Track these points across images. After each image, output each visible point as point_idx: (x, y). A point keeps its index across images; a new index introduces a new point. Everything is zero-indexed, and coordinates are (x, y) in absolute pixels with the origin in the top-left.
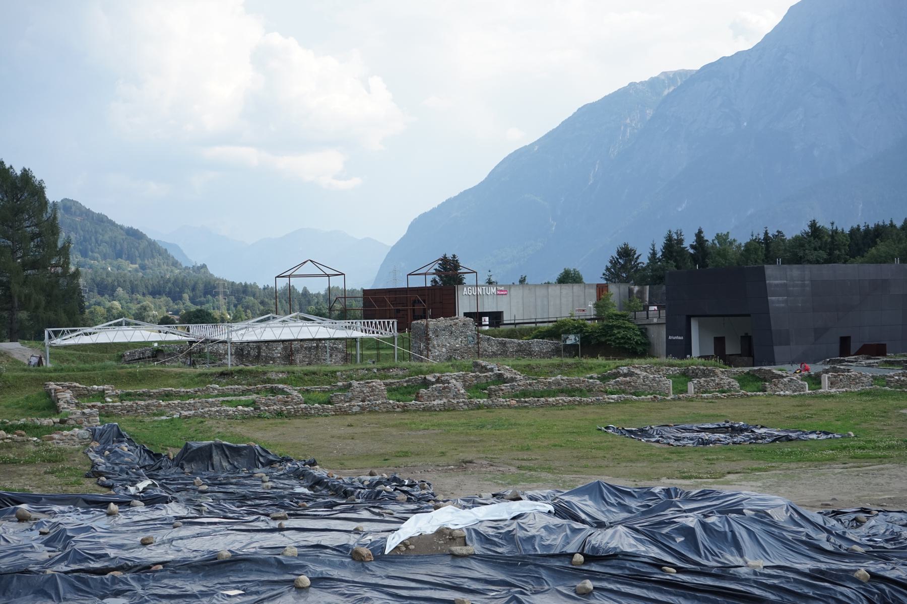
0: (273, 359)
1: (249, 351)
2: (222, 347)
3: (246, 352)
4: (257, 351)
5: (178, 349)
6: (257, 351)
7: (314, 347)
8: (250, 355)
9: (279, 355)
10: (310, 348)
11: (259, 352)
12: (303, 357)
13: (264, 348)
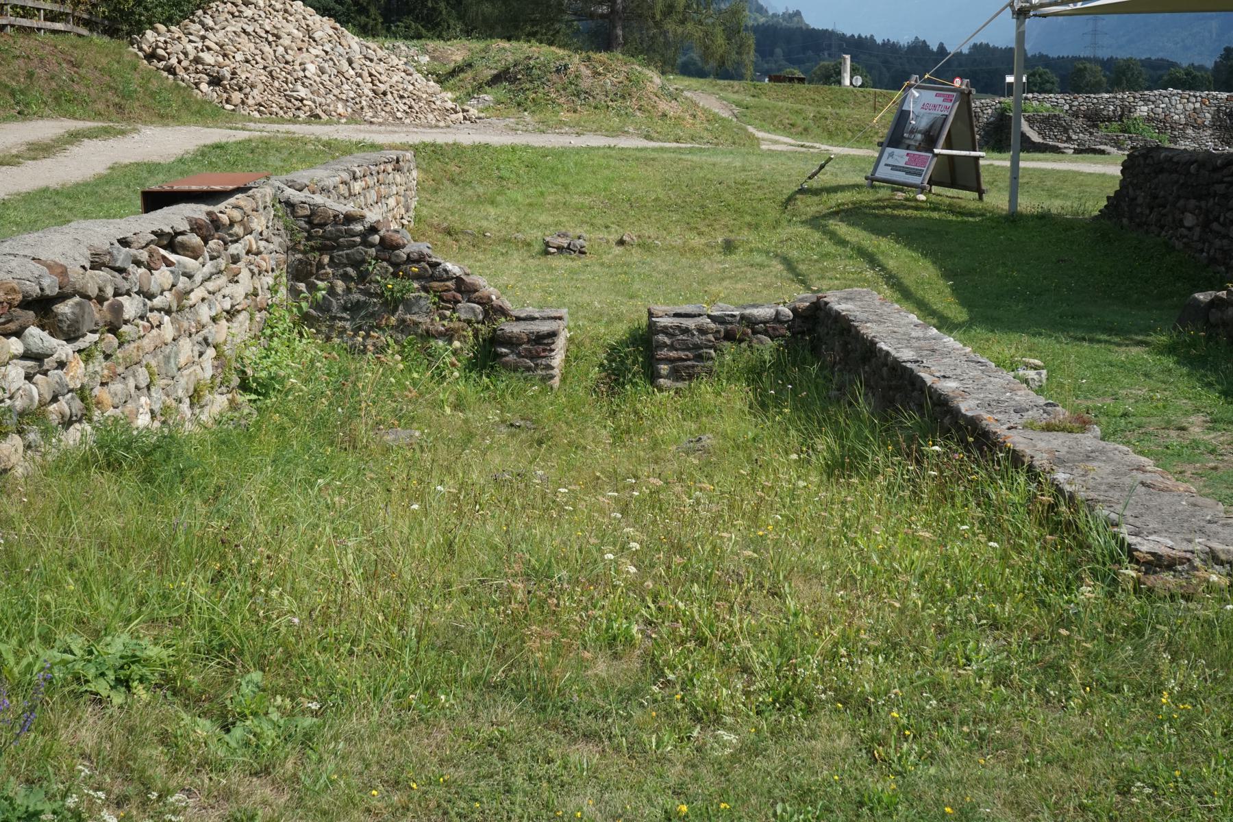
5: (1067, 107)
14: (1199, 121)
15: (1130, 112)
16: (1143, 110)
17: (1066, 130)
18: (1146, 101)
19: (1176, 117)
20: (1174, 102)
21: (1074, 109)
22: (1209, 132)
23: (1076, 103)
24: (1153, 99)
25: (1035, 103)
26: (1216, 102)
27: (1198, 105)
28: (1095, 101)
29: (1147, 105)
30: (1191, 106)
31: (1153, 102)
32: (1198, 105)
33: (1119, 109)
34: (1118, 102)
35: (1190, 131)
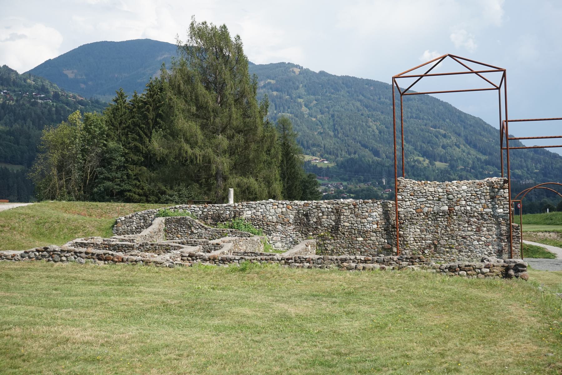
0: (364, 233)
1: (319, 218)
2: (272, 211)
3: (315, 220)
4: (333, 218)
5: (200, 212)
6: (333, 218)
7: (443, 212)
8: (321, 225)
9: (375, 226)
10: (436, 214)
11: (338, 221)
12: (422, 231)
13: (347, 213)
14: (286, 220)
15: (240, 215)
16: (248, 214)
17: (190, 227)
18: (250, 207)
19: (270, 218)
20: (268, 208)
21: (205, 213)
22: (292, 227)
23: (206, 210)
24: (254, 206)
25: (181, 211)
26: (296, 207)
27: (284, 210)
28: (218, 208)
29: (251, 210)
30: (280, 210)
31: (255, 208)
32: (284, 210)
33: (232, 212)
34: (232, 209)
35: (279, 227)
